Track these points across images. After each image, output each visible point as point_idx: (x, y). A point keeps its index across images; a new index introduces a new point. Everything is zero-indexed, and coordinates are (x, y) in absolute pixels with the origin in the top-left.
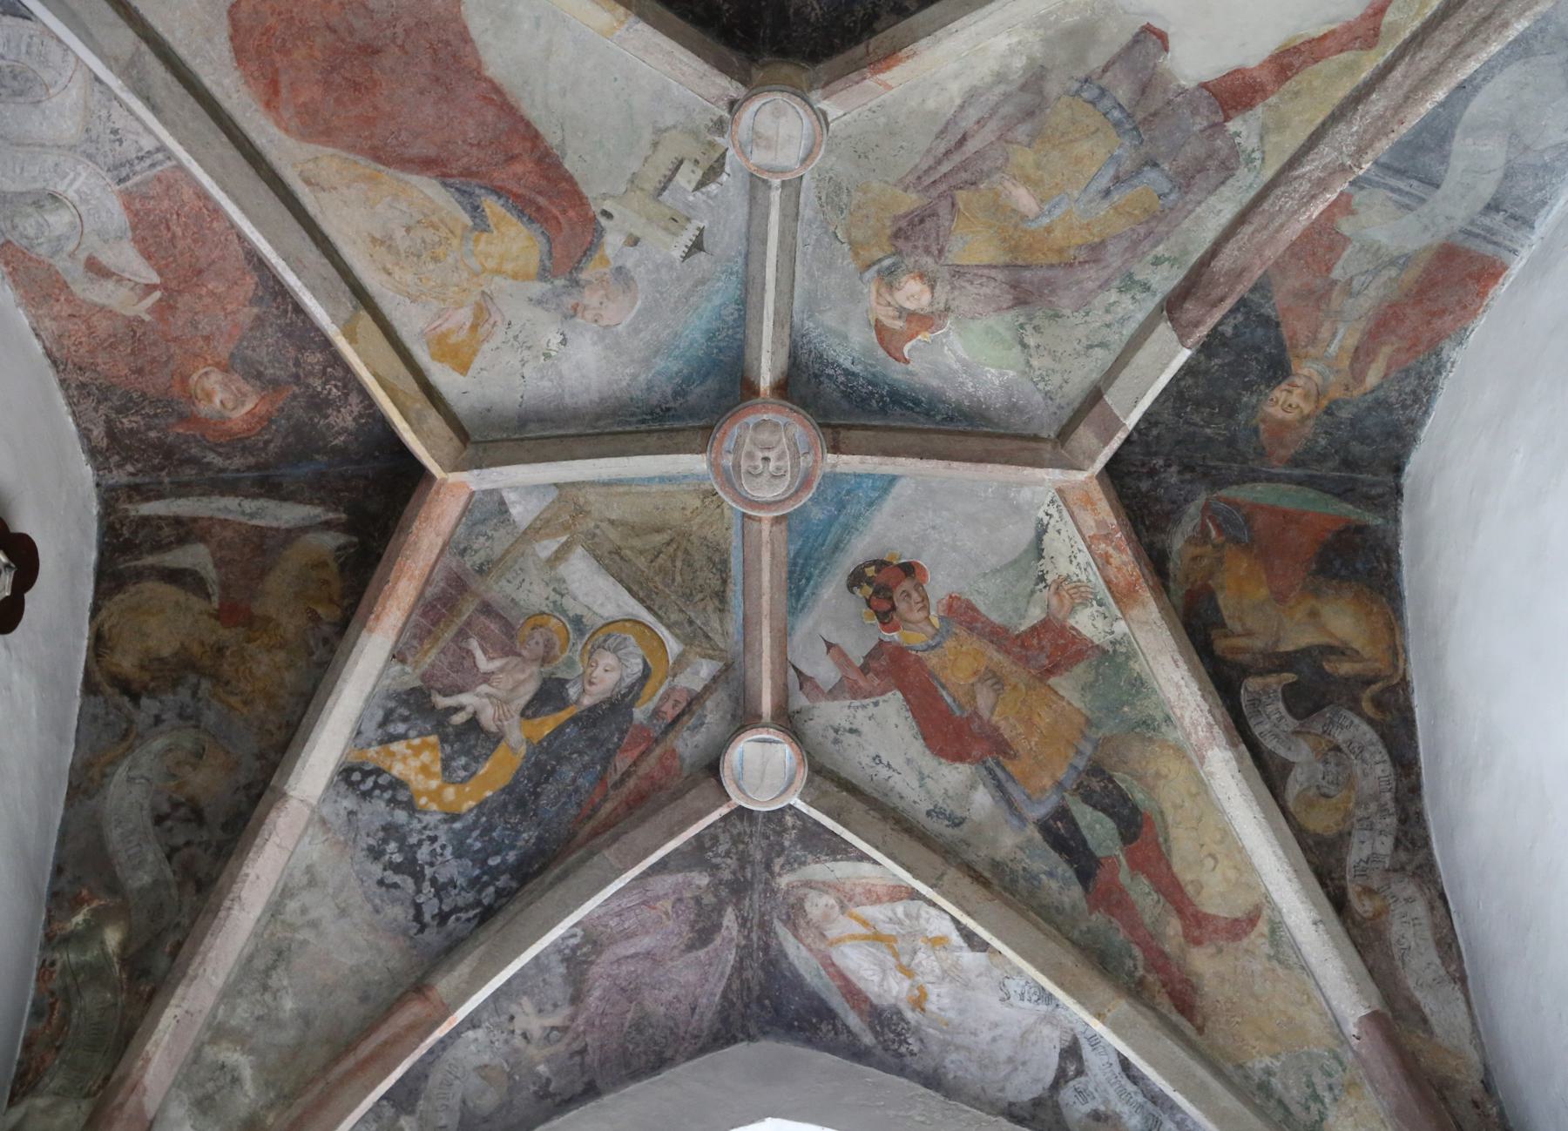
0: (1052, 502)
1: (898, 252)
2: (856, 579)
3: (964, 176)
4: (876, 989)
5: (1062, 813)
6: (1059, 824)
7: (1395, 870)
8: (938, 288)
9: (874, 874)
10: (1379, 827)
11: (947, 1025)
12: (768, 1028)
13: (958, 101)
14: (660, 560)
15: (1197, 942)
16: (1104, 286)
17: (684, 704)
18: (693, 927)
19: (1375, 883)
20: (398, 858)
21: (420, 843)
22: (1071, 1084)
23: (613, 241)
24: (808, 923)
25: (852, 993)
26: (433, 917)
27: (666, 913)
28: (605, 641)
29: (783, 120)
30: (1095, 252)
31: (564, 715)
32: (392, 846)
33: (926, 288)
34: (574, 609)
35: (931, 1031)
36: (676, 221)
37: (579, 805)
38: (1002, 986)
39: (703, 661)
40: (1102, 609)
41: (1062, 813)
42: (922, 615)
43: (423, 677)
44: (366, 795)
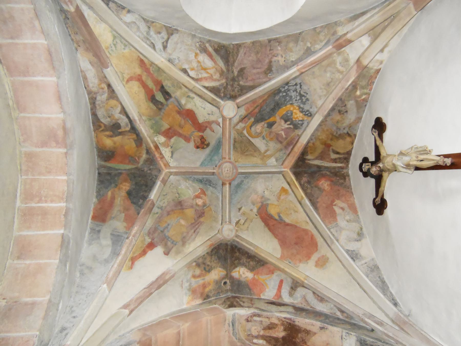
0: (170, 163)
1: (204, 210)
2: (208, 145)
3: (194, 225)
5: (167, 100)
6: (167, 97)
7: (96, 93)
8: (195, 204)
10: (100, 102)
12: (228, 46)
13: (196, 238)
14: (247, 149)
15: (139, 75)
16: (166, 207)
17: (243, 120)
19: (101, 91)
20: (303, 98)
21: (299, 100)
22: (165, 40)
23: (255, 210)
25: (210, 56)
26: (298, 85)
27: (250, 77)
28: (258, 134)
30: (168, 214)
31: (268, 121)
32: (304, 100)
33: (198, 203)
34: (264, 141)
35: (194, 49)
36: (244, 214)
37: (266, 103)
38: (179, 61)
39: (239, 129)
40: (159, 142)
41: (167, 100)
42: (195, 139)
43: (294, 131)
44: (308, 111)
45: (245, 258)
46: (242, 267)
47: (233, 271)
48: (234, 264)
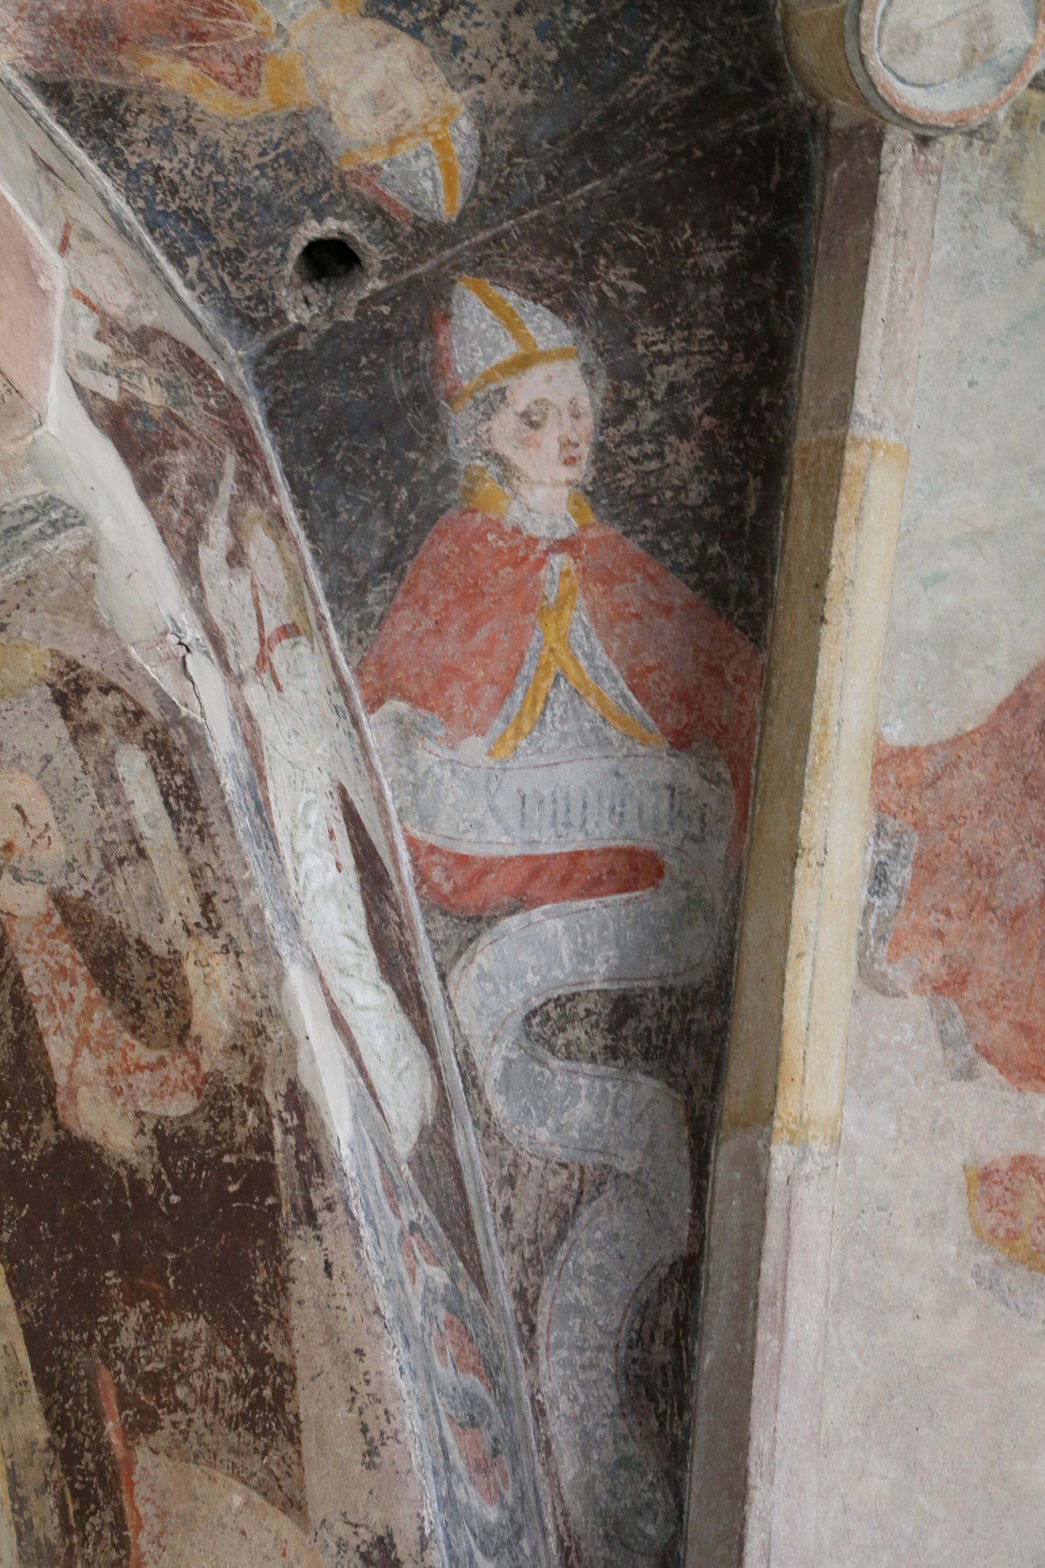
29: (919, 24)
45: (700, 362)
46: (588, 372)
47: (498, 291)
48: (587, 272)
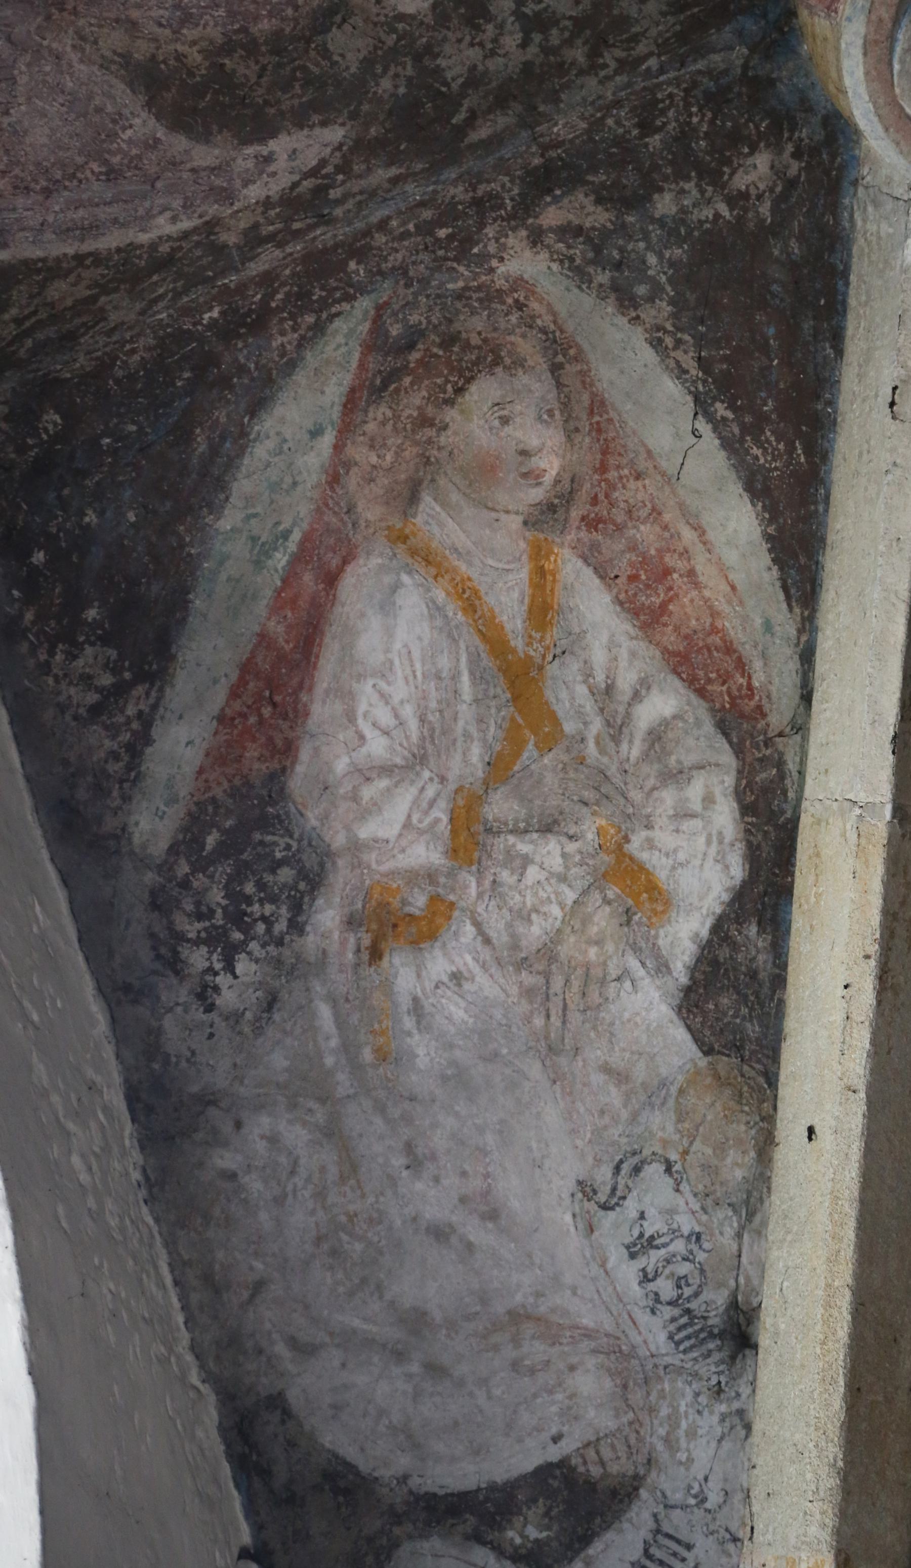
4: (341, 765)
9: (731, 557)
11: (382, 1055)
18: (227, 48)
24: (424, 421)
35: (325, 1012)
